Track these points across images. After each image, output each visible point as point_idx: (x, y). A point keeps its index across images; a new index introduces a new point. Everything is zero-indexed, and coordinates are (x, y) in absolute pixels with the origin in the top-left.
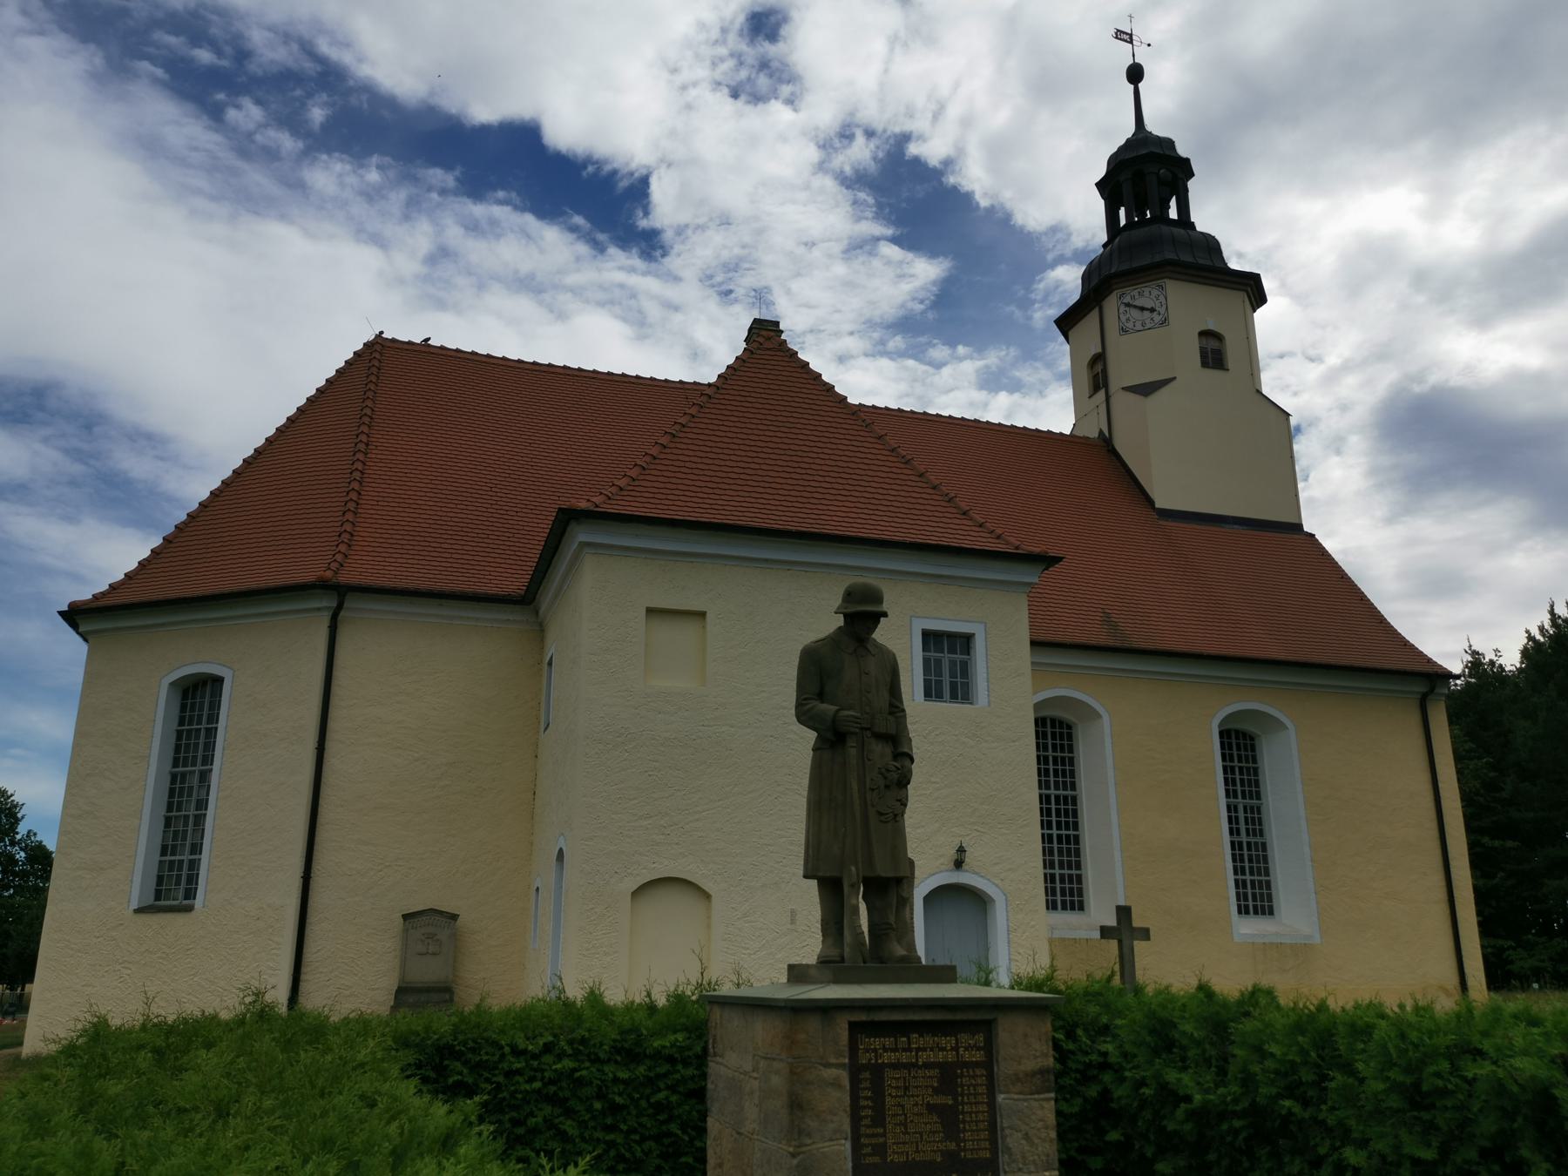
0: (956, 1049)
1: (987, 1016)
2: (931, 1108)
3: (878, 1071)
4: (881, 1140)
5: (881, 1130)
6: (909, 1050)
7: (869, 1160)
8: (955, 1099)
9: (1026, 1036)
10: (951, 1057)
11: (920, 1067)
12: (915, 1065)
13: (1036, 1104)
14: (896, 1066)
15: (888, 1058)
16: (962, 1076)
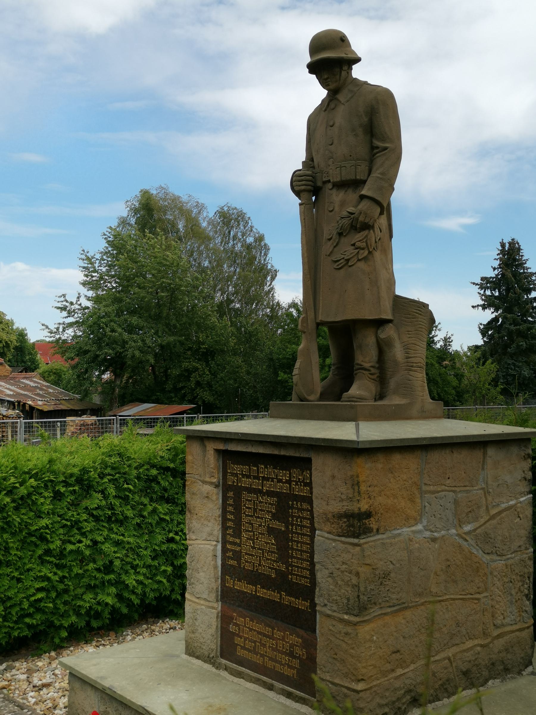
0: (289, 482)
1: (304, 455)
2: (271, 531)
3: (238, 491)
4: (238, 549)
5: (238, 541)
6: (257, 478)
7: (231, 562)
8: (287, 527)
9: (333, 477)
10: (285, 488)
11: (264, 494)
12: (260, 492)
13: (340, 546)
14: (250, 490)
15: (245, 482)
16: (292, 507)
